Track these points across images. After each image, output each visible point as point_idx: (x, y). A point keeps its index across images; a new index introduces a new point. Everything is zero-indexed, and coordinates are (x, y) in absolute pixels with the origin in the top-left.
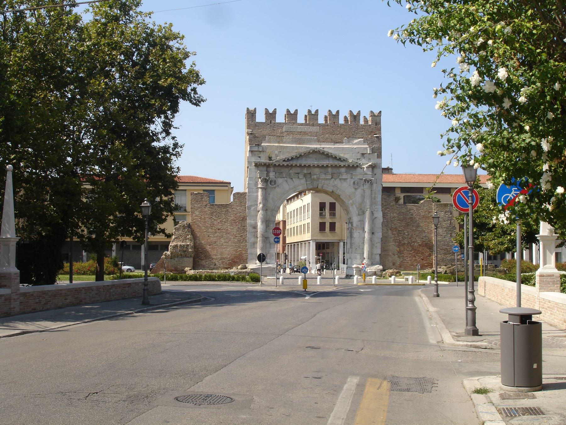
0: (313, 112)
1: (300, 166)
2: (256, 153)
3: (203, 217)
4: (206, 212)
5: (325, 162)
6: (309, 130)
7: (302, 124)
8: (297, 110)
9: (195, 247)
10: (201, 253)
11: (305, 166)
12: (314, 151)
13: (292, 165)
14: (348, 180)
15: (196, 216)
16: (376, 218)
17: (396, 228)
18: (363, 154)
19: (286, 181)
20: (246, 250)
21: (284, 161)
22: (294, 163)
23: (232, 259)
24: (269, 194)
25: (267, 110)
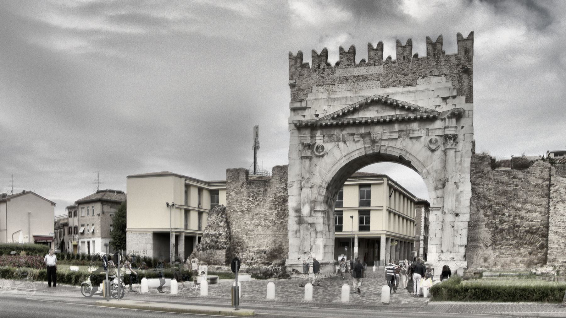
3: (239, 199)
4: (242, 192)
6: (370, 73)
13: (343, 124)
14: (422, 139)
15: (232, 198)
16: (461, 192)
17: (491, 206)
20: (287, 241)
21: (333, 118)
23: (271, 253)
24: (316, 165)
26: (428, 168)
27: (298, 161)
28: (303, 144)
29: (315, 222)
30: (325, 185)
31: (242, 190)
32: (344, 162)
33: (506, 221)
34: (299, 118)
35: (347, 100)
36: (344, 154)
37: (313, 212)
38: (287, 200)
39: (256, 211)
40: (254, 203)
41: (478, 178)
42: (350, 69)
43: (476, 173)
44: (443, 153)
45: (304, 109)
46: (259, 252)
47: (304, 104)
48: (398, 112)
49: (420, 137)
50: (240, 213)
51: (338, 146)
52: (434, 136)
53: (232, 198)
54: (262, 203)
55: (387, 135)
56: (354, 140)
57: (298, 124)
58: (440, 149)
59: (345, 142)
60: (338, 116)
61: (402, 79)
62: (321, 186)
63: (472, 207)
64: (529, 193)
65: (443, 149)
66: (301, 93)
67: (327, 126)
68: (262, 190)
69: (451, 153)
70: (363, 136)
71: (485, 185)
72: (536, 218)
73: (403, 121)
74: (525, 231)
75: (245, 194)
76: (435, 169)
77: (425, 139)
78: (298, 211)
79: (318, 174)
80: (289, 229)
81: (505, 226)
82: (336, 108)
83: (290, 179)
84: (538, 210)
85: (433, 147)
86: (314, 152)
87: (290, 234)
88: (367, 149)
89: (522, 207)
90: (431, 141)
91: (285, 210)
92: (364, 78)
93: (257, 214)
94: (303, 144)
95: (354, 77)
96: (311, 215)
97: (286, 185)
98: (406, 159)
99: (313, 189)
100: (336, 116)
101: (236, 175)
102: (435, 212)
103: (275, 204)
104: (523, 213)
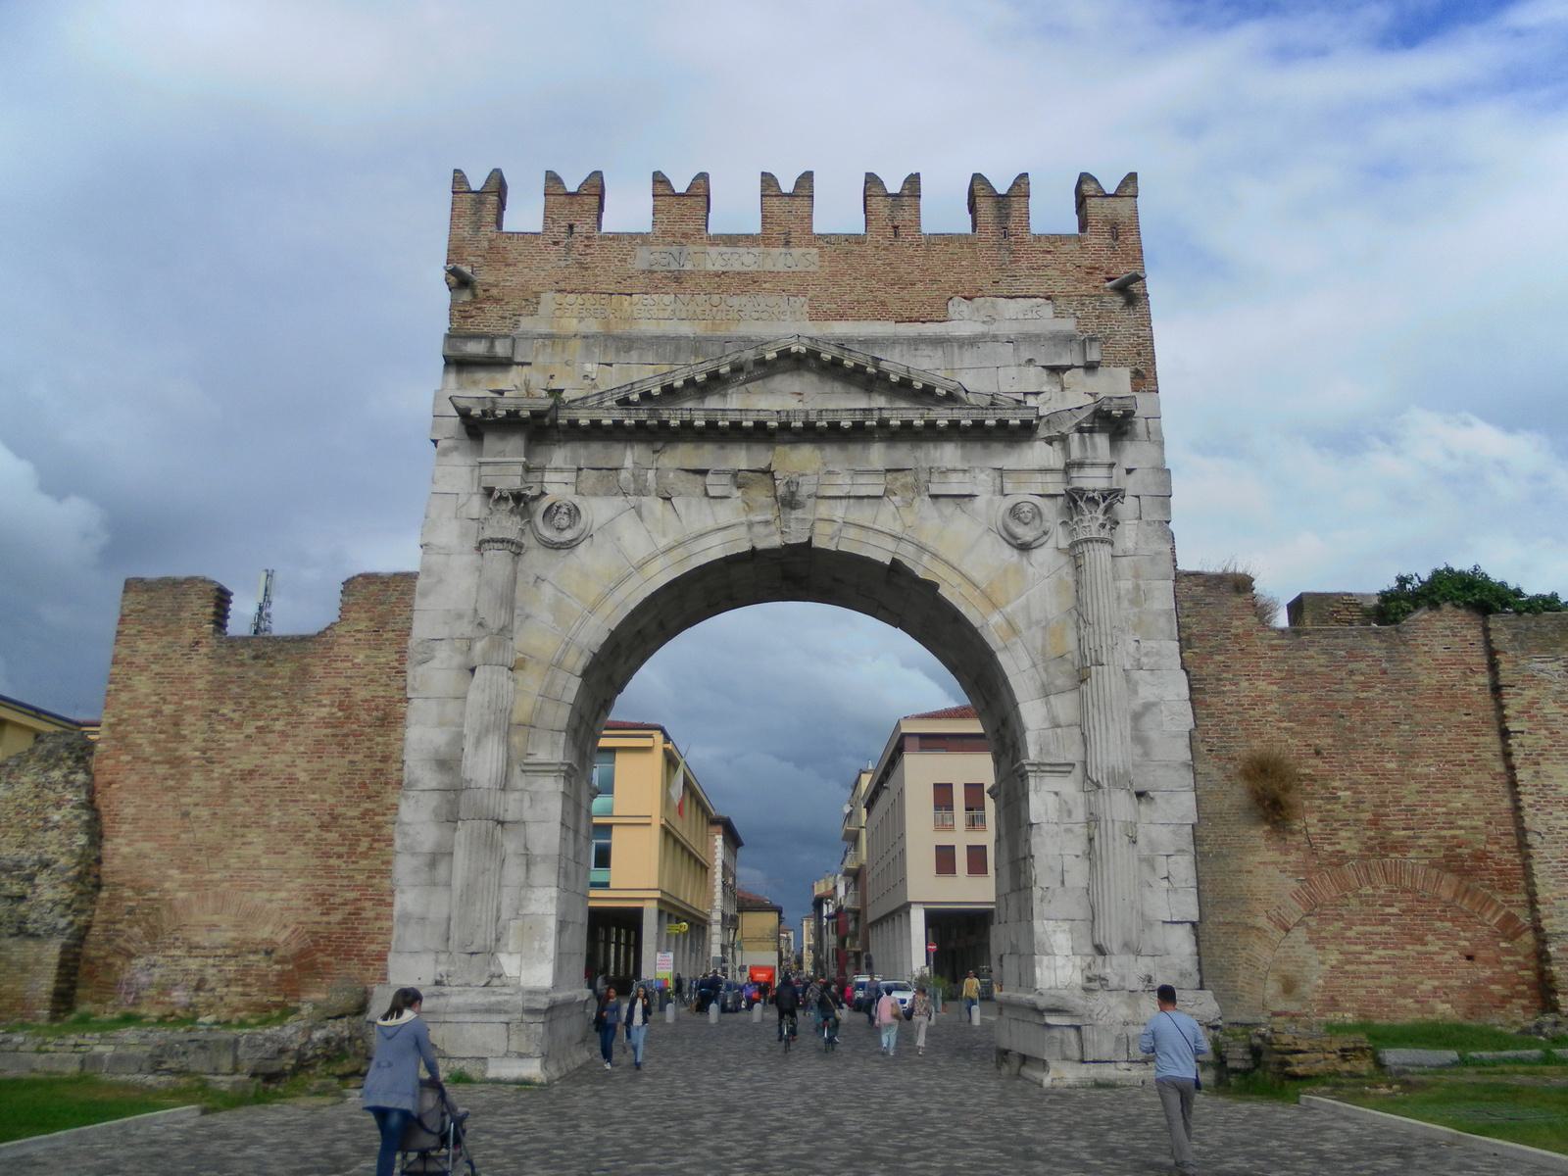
0: (787, 186)
1: (711, 425)
2: (481, 376)
3: (168, 709)
4: (187, 679)
5: (844, 404)
6: (768, 267)
7: (732, 240)
8: (703, 177)
9: (90, 878)
10: (131, 911)
11: (736, 426)
12: (785, 355)
13: (664, 425)
16: (1148, 707)
18: (1055, 370)
19: (638, 510)
20: (384, 901)
21: (624, 402)
23: (303, 953)
25: (553, 179)
26: (1009, 609)
27: (463, 561)
28: (489, 492)
29: (528, 815)
30: (578, 662)
31: (194, 668)
32: (660, 575)
33: (1346, 824)
34: (478, 390)
35: (678, 349)
37: (517, 770)
38: (403, 717)
39: (246, 763)
40: (239, 726)
41: (1211, 654)
43: (1202, 637)
44: (1064, 559)
45: (505, 364)
46: (237, 951)
47: (501, 349)
48: (879, 401)
49: (971, 496)
50: (161, 770)
51: (638, 510)
52: (1024, 493)
53: (136, 704)
54: (279, 726)
55: (843, 484)
56: (706, 494)
57: (476, 412)
58: (1051, 544)
59: (669, 499)
60: (646, 396)
62: (558, 664)
63: (1200, 768)
64: (1418, 717)
65: (1064, 544)
66: (492, 311)
67: (596, 432)
68: (285, 669)
69: (1098, 557)
70: (739, 480)
71: (1244, 684)
72: (1465, 812)
73: (906, 434)
74: (1433, 865)
75: (200, 684)
76: (1036, 615)
77: (990, 502)
78: (447, 763)
80: (398, 843)
81: (1348, 842)
82: (644, 373)
84: (1468, 781)
85: (1026, 534)
86: (534, 530)
87: (404, 867)
88: (759, 530)
89: (1400, 769)
90: (1014, 512)
91: (385, 759)
93: (248, 775)
94: (489, 492)
95: (707, 275)
96: (505, 786)
97: (402, 654)
98: (921, 573)
99: (519, 675)
100: (635, 397)
101: (168, 602)
102: (1052, 783)
103: (343, 732)
104: (1409, 793)
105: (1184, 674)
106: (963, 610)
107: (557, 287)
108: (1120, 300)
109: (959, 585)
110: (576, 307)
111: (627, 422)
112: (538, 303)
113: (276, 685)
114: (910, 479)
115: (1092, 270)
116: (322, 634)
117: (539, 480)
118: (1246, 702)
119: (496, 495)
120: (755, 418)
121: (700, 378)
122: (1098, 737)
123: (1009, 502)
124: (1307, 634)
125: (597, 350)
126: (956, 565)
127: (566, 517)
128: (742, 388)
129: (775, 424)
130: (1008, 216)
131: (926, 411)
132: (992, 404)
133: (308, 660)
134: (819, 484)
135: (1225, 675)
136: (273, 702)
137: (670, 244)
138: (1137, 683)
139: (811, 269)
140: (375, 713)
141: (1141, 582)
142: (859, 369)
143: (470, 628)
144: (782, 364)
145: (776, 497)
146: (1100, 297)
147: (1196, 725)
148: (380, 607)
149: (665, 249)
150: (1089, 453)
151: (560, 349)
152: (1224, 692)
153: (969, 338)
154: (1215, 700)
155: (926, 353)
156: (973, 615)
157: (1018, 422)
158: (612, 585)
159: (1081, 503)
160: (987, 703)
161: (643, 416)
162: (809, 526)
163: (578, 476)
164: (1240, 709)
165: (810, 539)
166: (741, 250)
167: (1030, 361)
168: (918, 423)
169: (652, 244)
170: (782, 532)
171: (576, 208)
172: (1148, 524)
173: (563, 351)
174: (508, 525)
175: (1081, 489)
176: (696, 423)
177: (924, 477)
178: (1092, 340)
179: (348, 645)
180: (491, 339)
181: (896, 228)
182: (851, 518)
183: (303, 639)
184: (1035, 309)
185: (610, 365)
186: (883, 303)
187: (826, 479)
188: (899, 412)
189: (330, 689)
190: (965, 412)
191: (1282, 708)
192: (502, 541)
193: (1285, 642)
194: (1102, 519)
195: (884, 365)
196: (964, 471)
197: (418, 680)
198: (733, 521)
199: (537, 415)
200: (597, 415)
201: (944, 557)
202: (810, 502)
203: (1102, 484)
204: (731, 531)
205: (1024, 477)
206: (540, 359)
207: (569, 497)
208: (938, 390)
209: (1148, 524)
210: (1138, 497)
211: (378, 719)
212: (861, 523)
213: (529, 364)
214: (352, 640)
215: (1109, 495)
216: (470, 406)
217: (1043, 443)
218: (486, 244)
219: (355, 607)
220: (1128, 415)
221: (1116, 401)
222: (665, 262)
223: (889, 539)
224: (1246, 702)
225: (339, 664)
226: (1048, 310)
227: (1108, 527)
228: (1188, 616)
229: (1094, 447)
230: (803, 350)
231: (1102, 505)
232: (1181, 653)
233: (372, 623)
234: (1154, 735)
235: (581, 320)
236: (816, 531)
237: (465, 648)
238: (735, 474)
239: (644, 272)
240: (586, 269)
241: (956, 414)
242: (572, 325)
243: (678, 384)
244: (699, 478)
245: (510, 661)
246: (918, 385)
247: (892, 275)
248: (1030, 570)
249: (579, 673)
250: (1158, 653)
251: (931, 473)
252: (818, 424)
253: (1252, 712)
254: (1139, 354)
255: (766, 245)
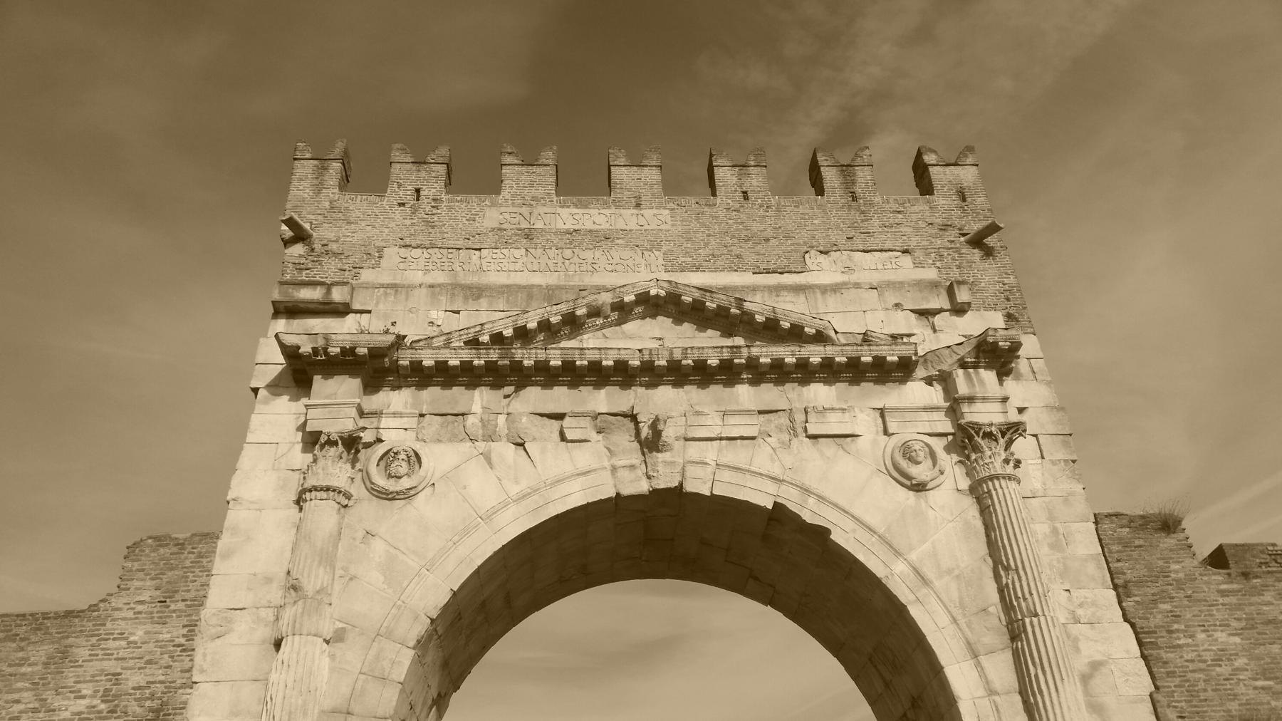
5: (709, 344)
13: (517, 367)
16: (1096, 666)
18: (923, 313)
21: (474, 343)
22: (527, 357)
32: (513, 525)
35: (530, 297)
36: (514, 490)
38: (184, 706)
42: (541, 210)
43: (1140, 583)
45: (342, 310)
47: (338, 295)
56: (563, 437)
59: (522, 445)
60: (498, 339)
61: (747, 251)
68: (40, 653)
70: (602, 423)
73: (779, 373)
77: (875, 442)
79: (376, 577)
83: (218, 597)
85: (920, 472)
88: (624, 474)
92: (602, 239)
95: (559, 232)
97: (192, 628)
98: (808, 517)
99: (338, 648)
100: (485, 338)
105: (1128, 626)
106: (861, 557)
107: (402, 243)
108: (977, 254)
109: (854, 531)
110: (422, 261)
111: (476, 362)
112: (380, 257)
113: (24, 674)
114: (783, 420)
115: (945, 228)
116: (94, 608)
117: (375, 425)
118: (1208, 656)
119: (323, 439)
120: (616, 357)
121: (555, 320)
122: (1048, 703)
123: (894, 441)
124: (1257, 577)
125: (443, 298)
126: (847, 508)
127: (404, 464)
128: (599, 333)
129: (637, 363)
130: (853, 183)
131: (797, 349)
132: (865, 340)
133: (71, 640)
134: (687, 426)
135: (1176, 626)
136: (16, 696)
137: (519, 206)
138: (1076, 640)
139: (663, 227)
140: (148, 703)
141: (1058, 525)
142: (722, 312)
143: (280, 593)
144: (639, 310)
145: (640, 442)
146: (958, 250)
147: (1157, 688)
148: (170, 574)
149: (515, 210)
150: (978, 389)
151: (403, 296)
152: (1179, 646)
153: (831, 285)
154: (1171, 655)
155: (788, 299)
156: (874, 565)
157: (896, 358)
158: (456, 538)
159: (979, 440)
160: (887, 685)
161: (494, 355)
162: (679, 469)
163: (419, 423)
164: (1202, 666)
165: (681, 484)
166: (592, 211)
167: (897, 305)
168: (790, 360)
169: (501, 205)
170: (649, 477)
171: (423, 174)
172: (1053, 463)
173: (407, 299)
174: (335, 470)
175: (977, 424)
176: (552, 363)
177: (800, 417)
178: (959, 283)
179: (124, 619)
180: (329, 287)
181: (745, 192)
182: (724, 460)
183: (69, 614)
184: (894, 260)
185: (458, 312)
186: (739, 257)
187: (693, 420)
188: (766, 353)
189: (93, 676)
190: (838, 348)
191: (1252, 663)
192: (328, 489)
193: (1235, 586)
194: (1003, 456)
195: (747, 306)
196: (843, 410)
197: (209, 658)
198: (594, 466)
199: (377, 354)
200: (444, 355)
201: (834, 499)
202: (678, 445)
203: (998, 419)
204: (588, 477)
205: (908, 416)
206: (381, 306)
207: (409, 444)
208: (807, 329)
209: (1053, 463)
210: (1035, 436)
211: (151, 710)
212: (737, 465)
213: (369, 312)
214: (130, 614)
215: (1008, 429)
216: (299, 343)
217: (922, 383)
218: (327, 204)
219: (141, 575)
220: (1015, 346)
221: (1002, 333)
222: (514, 221)
223: (769, 482)
224: (1208, 656)
225: (111, 644)
226: (906, 261)
227: (1012, 464)
228: (1119, 561)
229: (982, 382)
230: (663, 293)
231: (1002, 441)
232: (1120, 603)
233: (158, 593)
234: (1109, 700)
235: (427, 271)
236: (688, 474)
237: (272, 619)
238: (596, 416)
239: (493, 230)
240: (433, 227)
241: (829, 351)
242: (417, 277)
243: (532, 325)
244: (555, 424)
245: (328, 629)
246: (786, 325)
247: (746, 233)
248: (931, 512)
249: (412, 644)
250: (1094, 604)
251: (806, 413)
252: (684, 362)
253: (1218, 669)
254: (1008, 299)
255: (618, 207)
